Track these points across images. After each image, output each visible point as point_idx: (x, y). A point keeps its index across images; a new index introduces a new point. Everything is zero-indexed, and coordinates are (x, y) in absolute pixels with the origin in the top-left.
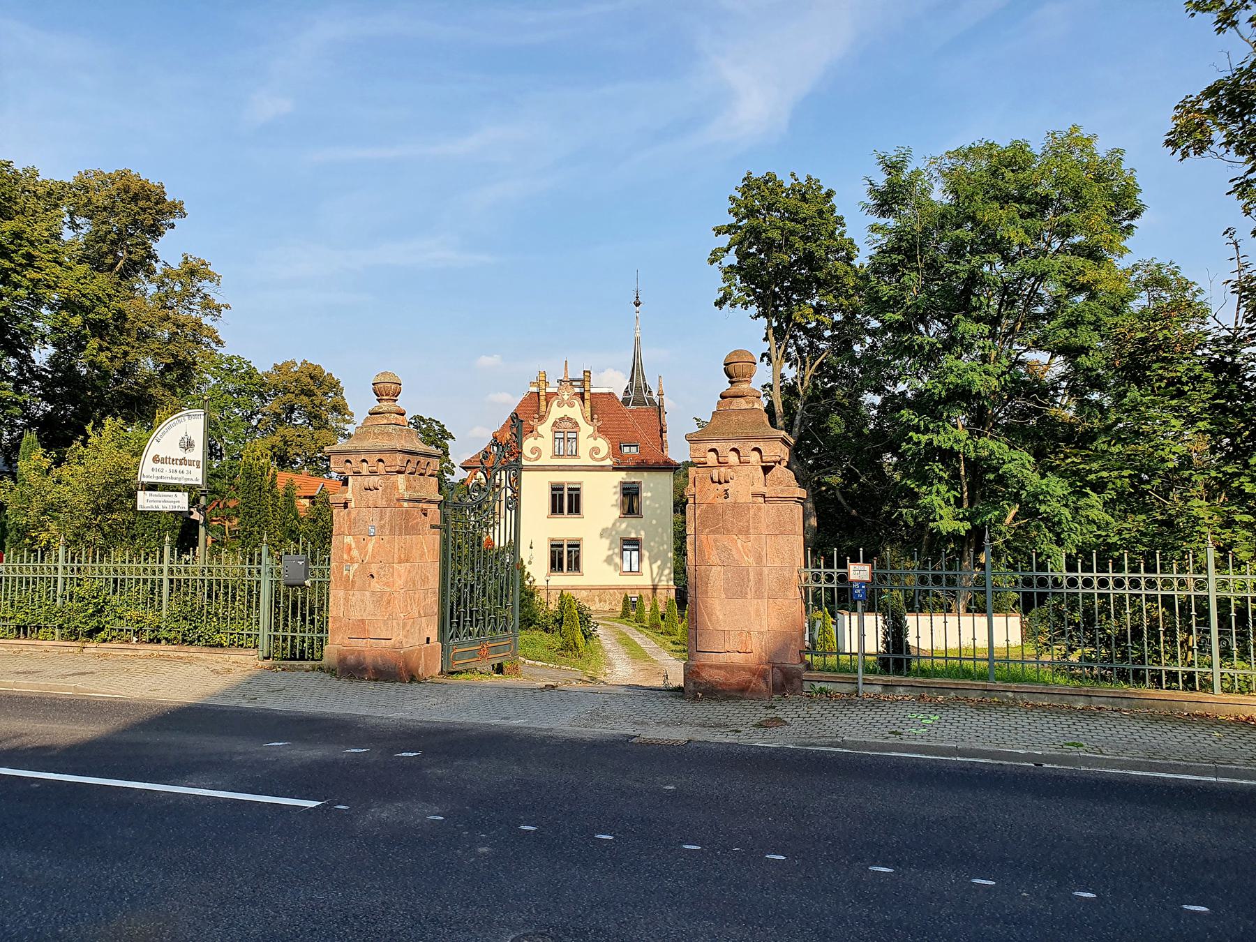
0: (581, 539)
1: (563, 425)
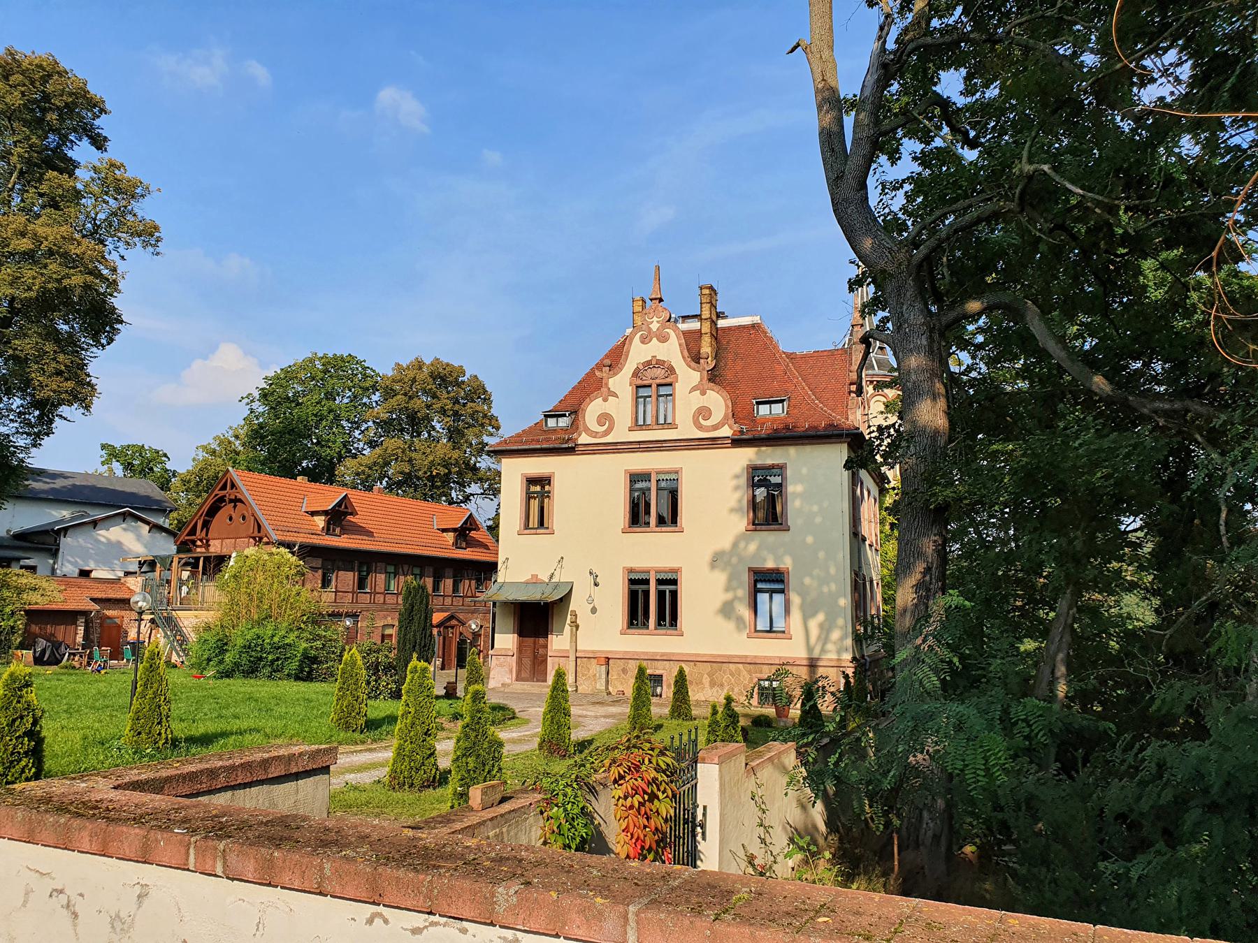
0: (676, 571)
1: (651, 373)
